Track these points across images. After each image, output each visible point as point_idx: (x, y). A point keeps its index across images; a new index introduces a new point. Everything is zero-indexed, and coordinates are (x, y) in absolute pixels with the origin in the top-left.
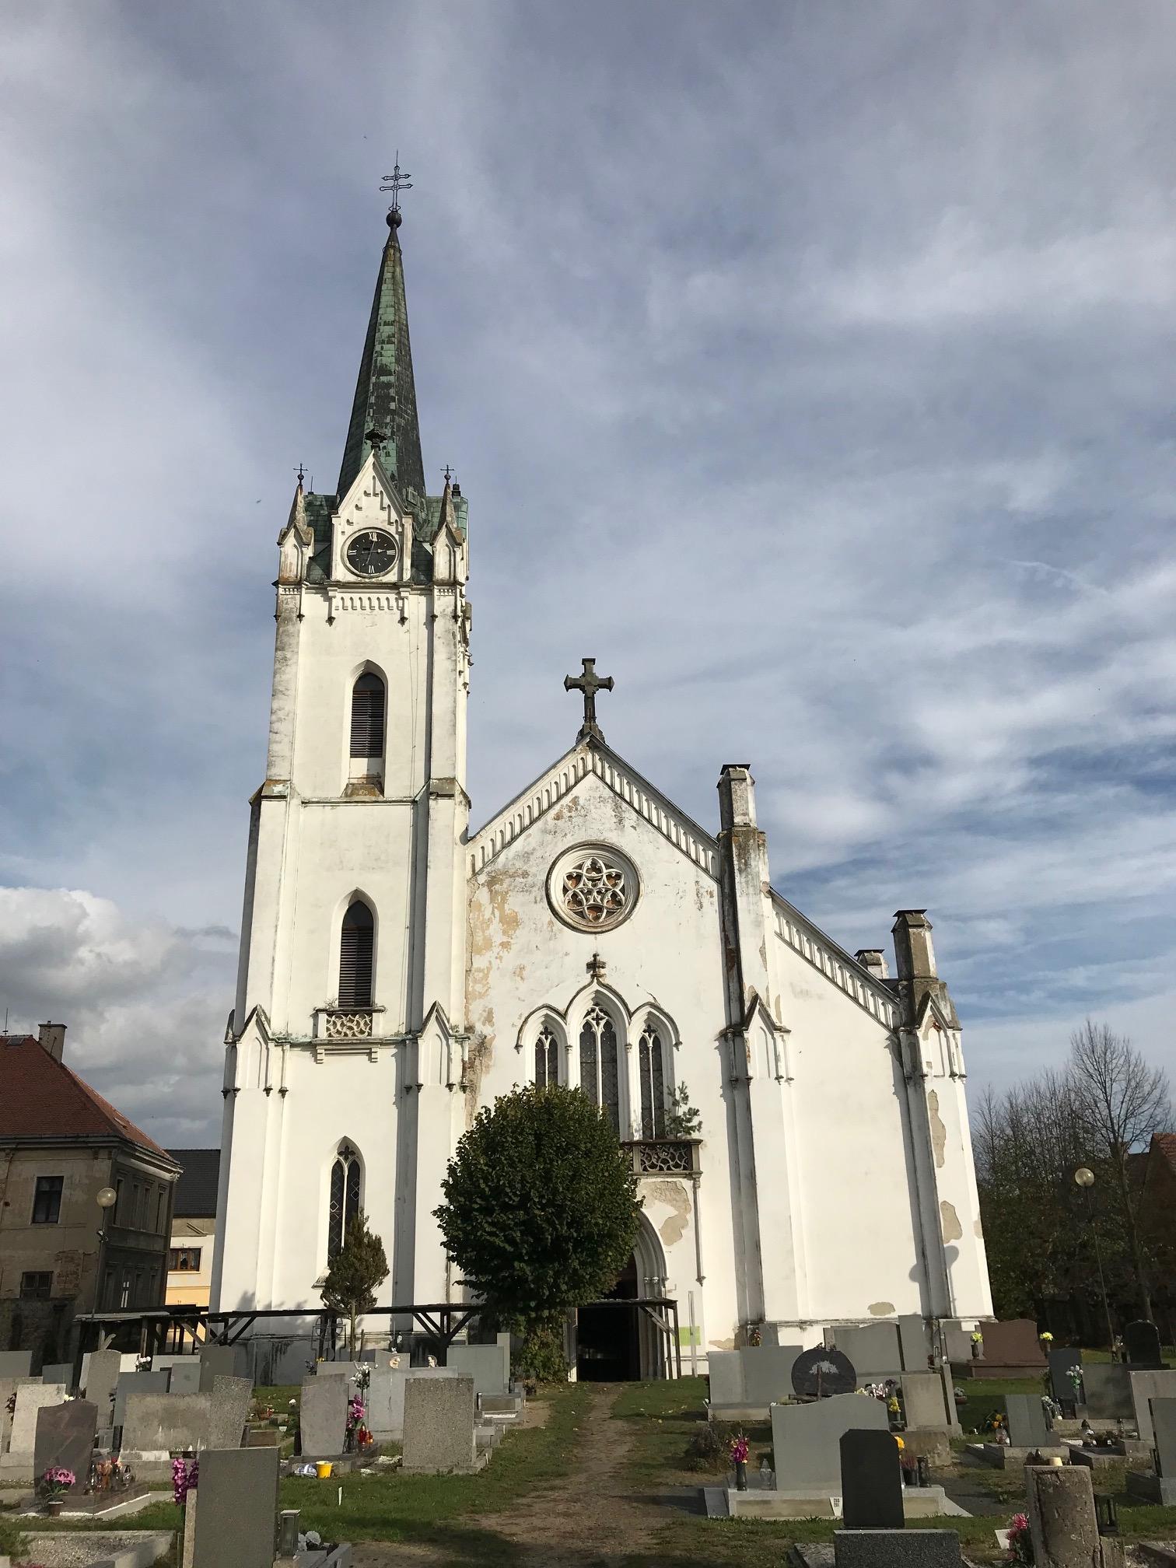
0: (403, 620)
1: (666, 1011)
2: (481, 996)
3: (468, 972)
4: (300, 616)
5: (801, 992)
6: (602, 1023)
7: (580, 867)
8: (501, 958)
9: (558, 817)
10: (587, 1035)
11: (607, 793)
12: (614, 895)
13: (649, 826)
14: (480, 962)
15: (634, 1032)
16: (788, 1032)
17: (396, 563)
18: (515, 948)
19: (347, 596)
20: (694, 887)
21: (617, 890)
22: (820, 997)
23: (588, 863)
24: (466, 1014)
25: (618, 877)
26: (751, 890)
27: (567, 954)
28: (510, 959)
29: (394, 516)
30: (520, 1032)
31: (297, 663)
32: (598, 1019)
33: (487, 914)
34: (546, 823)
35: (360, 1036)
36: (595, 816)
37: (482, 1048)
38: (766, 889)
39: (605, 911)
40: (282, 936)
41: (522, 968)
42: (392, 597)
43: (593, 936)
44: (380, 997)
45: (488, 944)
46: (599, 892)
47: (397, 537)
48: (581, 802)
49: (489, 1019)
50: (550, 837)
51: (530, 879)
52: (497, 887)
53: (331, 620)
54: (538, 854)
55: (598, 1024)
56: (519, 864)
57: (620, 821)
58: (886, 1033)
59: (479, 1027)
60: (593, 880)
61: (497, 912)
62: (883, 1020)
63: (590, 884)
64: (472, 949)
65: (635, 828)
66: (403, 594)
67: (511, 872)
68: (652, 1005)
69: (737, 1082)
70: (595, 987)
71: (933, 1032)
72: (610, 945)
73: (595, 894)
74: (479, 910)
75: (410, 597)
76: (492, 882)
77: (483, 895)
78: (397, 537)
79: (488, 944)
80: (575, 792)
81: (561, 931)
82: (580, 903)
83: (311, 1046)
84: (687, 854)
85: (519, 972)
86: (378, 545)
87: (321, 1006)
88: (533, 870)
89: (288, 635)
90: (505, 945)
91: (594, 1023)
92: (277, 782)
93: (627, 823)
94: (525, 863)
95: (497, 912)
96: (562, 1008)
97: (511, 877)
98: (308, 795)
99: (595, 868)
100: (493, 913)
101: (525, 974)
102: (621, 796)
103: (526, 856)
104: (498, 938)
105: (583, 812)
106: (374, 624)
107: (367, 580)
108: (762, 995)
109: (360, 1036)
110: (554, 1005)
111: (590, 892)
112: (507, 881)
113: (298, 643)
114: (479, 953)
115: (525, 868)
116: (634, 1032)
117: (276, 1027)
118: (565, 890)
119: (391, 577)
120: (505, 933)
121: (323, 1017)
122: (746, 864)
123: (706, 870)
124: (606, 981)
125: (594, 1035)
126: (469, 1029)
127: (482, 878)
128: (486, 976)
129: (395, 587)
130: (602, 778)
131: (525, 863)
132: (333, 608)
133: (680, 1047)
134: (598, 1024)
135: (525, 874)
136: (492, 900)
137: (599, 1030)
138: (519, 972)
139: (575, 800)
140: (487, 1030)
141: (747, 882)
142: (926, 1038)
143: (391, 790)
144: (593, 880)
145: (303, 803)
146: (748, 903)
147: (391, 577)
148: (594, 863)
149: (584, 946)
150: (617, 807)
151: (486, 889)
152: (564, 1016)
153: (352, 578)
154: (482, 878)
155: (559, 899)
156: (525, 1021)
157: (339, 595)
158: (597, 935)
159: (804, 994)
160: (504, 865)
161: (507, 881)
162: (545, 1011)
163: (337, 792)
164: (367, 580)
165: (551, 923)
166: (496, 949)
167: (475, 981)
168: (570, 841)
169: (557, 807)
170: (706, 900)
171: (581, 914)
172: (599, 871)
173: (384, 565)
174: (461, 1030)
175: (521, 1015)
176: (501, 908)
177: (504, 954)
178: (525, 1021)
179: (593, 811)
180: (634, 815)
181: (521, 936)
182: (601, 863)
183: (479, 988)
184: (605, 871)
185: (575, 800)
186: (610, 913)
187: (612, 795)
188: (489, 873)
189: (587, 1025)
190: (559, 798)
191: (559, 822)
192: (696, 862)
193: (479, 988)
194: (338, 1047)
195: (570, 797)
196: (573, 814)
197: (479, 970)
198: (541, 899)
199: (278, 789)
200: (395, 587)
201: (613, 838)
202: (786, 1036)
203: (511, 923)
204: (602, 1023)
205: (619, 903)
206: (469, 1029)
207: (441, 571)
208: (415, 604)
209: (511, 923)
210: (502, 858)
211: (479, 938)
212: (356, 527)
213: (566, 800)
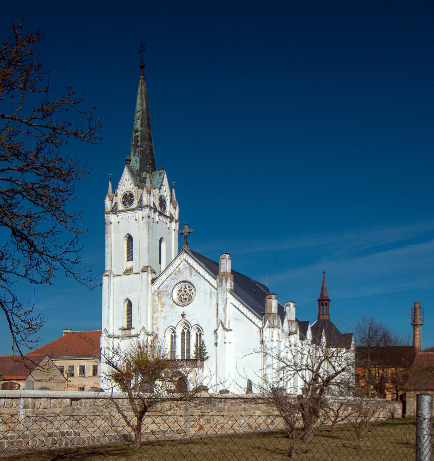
0: (136, 220)
1: (201, 326)
2: (156, 324)
3: (153, 318)
4: (111, 223)
5: (236, 319)
6: (187, 329)
7: (182, 288)
8: (160, 314)
9: (175, 274)
10: (183, 333)
11: (188, 266)
12: (190, 295)
13: (199, 275)
14: (155, 316)
15: (193, 333)
16: (231, 330)
18: (164, 311)
19: (122, 214)
20: (210, 292)
21: (191, 294)
22: (241, 320)
23: (184, 287)
24: (152, 328)
25: (191, 290)
26: (222, 292)
27: (176, 312)
28: (163, 314)
30: (165, 332)
31: (111, 237)
32: (186, 328)
33: (157, 303)
34: (172, 276)
35: (129, 335)
36: (184, 273)
37: (157, 336)
38: (228, 291)
39: (188, 300)
40: (111, 311)
41: (165, 317)
43: (183, 307)
44: (133, 325)
45: (158, 311)
46: (186, 295)
48: (181, 269)
49: (158, 329)
50: (173, 280)
51: (168, 293)
52: (159, 295)
53: (119, 222)
54: (170, 285)
56: (165, 289)
57: (191, 274)
58: (258, 329)
59: (155, 332)
60: (185, 291)
61: (159, 302)
62: (259, 326)
63: (184, 293)
64: (154, 312)
65: (195, 276)
66: (136, 212)
67: (163, 291)
68: (197, 324)
69: (216, 344)
70: (183, 320)
71: (268, 328)
72: (187, 309)
73: (185, 295)
74: (155, 302)
75: (138, 212)
76: (158, 294)
77: (156, 298)
78: (134, 193)
79: (158, 311)
80: (179, 267)
81: (175, 306)
82: (181, 298)
83: (118, 338)
84: (209, 282)
85: (165, 318)
86: (129, 196)
87: (120, 328)
88: (169, 290)
89: (108, 229)
90: (162, 311)
91: (185, 329)
92: (107, 271)
93: (193, 274)
94: (166, 288)
95: (159, 302)
96: (175, 326)
97: (163, 292)
98: (115, 274)
99: (185, 288)
100: (159, 302)
101: (166, 318)
102: (192, 267)
103: (167, 286)
104: (160, 309)
105: (181, 272)
106: (129, 222)
107: (127, 208)
108: (223, 321)
109: (129, 335)
110: (173, 325)
111: (184, 295)
112: (162, 293)
113: (111, 231)
114: (155, 313)
115: (166, 290)
116: (193, 333)
117: (111, 333)
118: (178, 294)
119: (133, 207)
120: (161, 307)
121: (121, 330)
122: (221, 284)
123: (214, 287)
124: (186, 319)
125: (185, 332)
126: (153, 332)
127: (156, 293)
128: (157, 319)
130: (187, 262)
131: (166, 288)
133: (204, 335)
135: (166, 291)
136: (158, 299)
137: (186, 331)
138: (165, 318)
139: (179, 269)
140: (157, 332)
141: (221, 290)
142: (266, 331)
143: (134, 271)
144: (185, 291)
145: (114, 276)
146: (221, 295)
147: (133, 207)
148: (185, 287)
149: (181, 310)
150: (190, 270)
151: (157, 296)
152: (175, 328)
154: (156, 293)
155: (175, 297)
156: (166, 330)
157: (120, 215)
158: (184, 307)
159: (237, 320)
160: (161, 289)
161: (162, 293)
162: (171, 327)
163: (122, 273)
164: (127, 208)
165: (173, 304)
166: (159, 312)
167: (154, 321)
168: (178, 281)
169: (175, 272)
170: (213, 296)
171: (181, 301)
172: (187, 288)
173: (131, 202)
174: (151, 332)
175: (165, 329)
176: (161, 301)
177: (161, 313)
178: (166, 330)
179: (184, 271)
180: (195, 272)
181: (166, 308)
182: (187, 287)
183: (155, 322)
184: (188, 288)
185: (179, 269)
186: (189, 300)
187: (189, 266)
188: (157, 292)
189: (183, 330)
190: (177, 268)
191: (175, 276)
192: (211, 284)
193: (155, 322)
194: (124, 337)
195: (178, 268)
196: (179, 273)
197: (155, 317)
198: (170, 298)
199: (107, 273)
201: (189, 279)
202: (230, 331)
203: (163, 305)
205: (191, 297)
206: (153, 332)
207: (145, 202)
208: (139, 214)
209: (163, 305)
210: (161, 287)
211: (155, 309)
212: (124, 192)
213: (177, 269)
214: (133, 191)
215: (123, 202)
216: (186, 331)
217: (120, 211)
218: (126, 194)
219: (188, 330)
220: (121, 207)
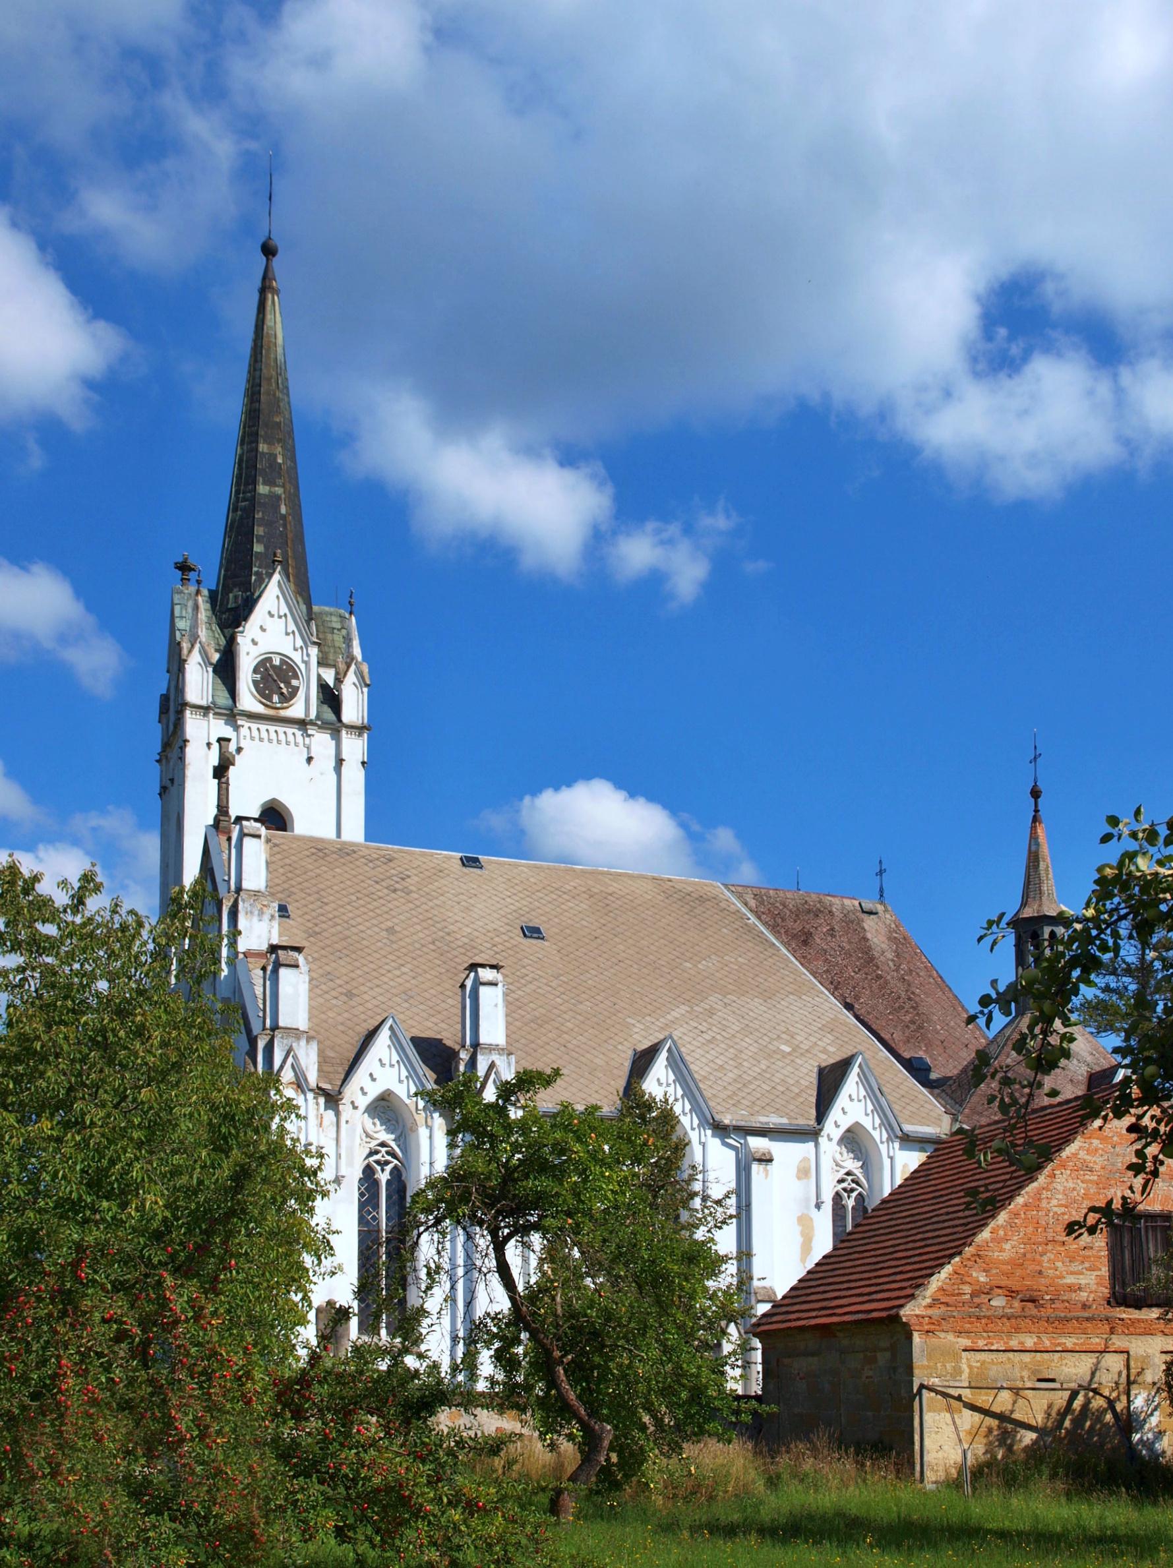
6: (388, 1168)
17: (301, 694)
19: (254, 726)
29: (299, 643)
42: (299, 733)
47: (302, 667)
55: (383, 1170)
66: (310, 732)
78: (302, 667)
119: (296, 710)
125: (376, 1183)
129: (302, 724)
132: (242, 737)
134: (383, 1170)
137: (384, 1177)
153: (259, 709)
157: (247, 725)
200: (302, 724)
204: (388, 1168)
214: (297, 657)
215: (255, 683)
216: (384, 1177)
217: (252, 716)
218: (270, 659)
219: (396, 1172)
220: (248, 700)
